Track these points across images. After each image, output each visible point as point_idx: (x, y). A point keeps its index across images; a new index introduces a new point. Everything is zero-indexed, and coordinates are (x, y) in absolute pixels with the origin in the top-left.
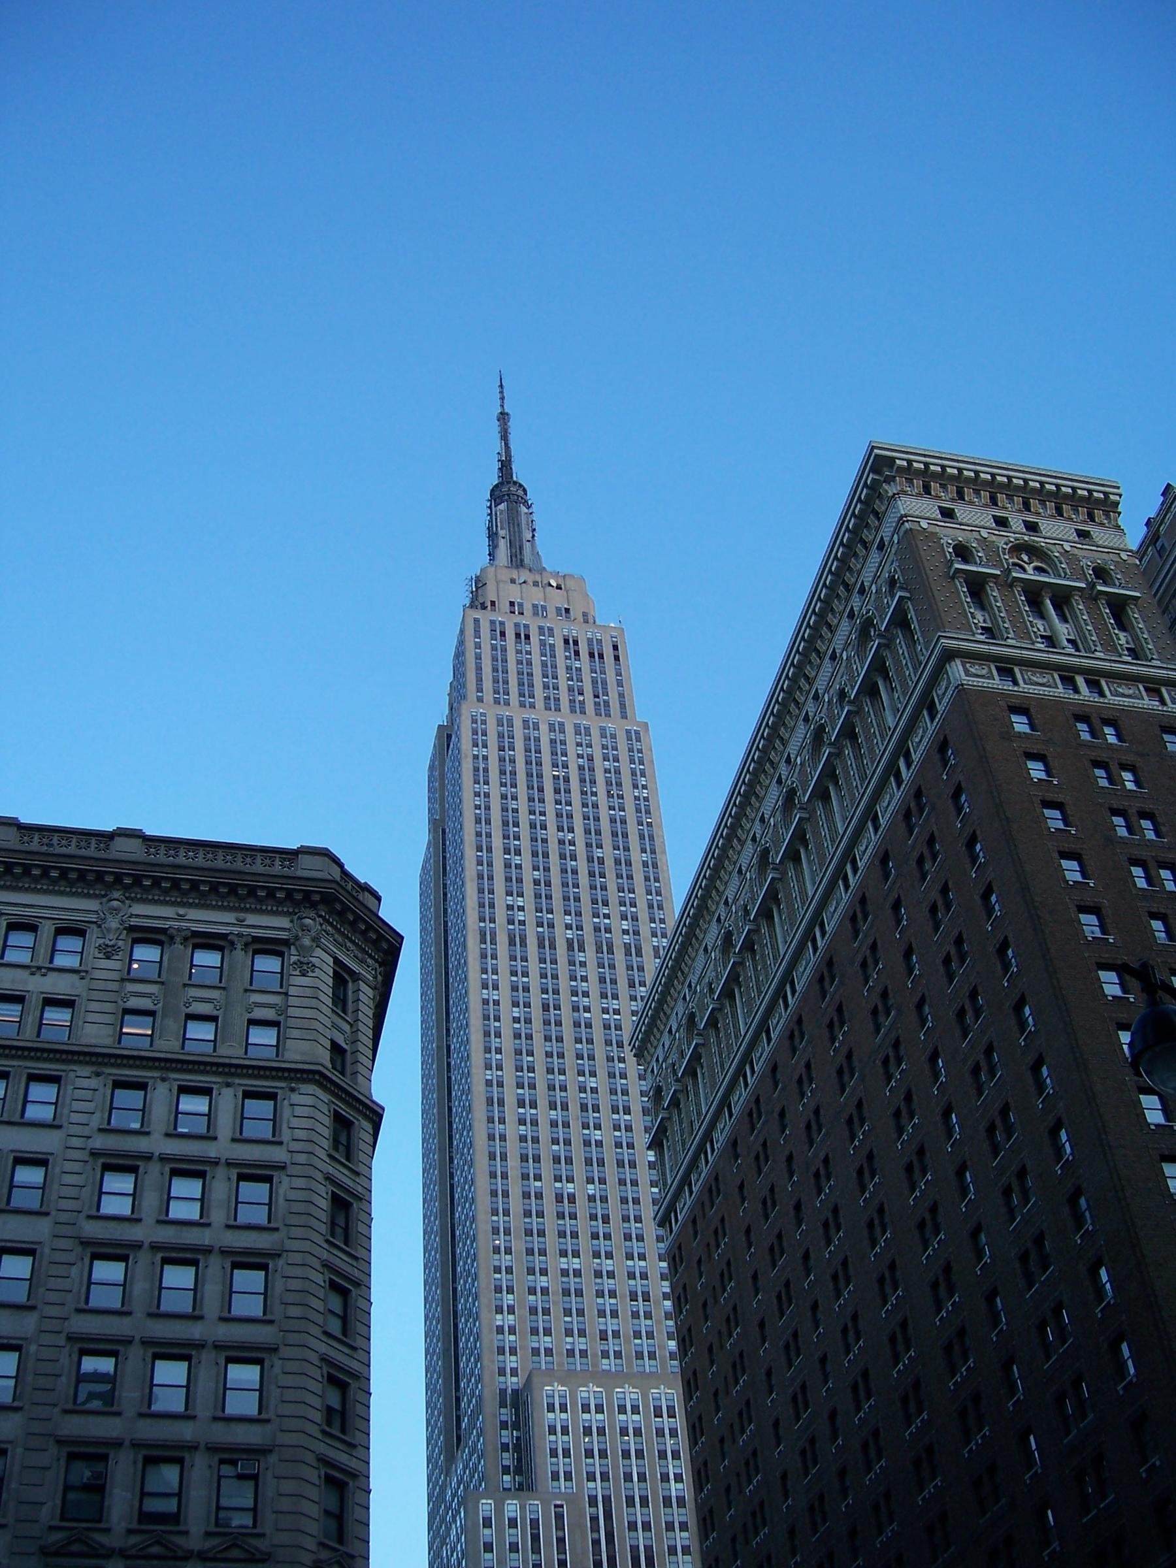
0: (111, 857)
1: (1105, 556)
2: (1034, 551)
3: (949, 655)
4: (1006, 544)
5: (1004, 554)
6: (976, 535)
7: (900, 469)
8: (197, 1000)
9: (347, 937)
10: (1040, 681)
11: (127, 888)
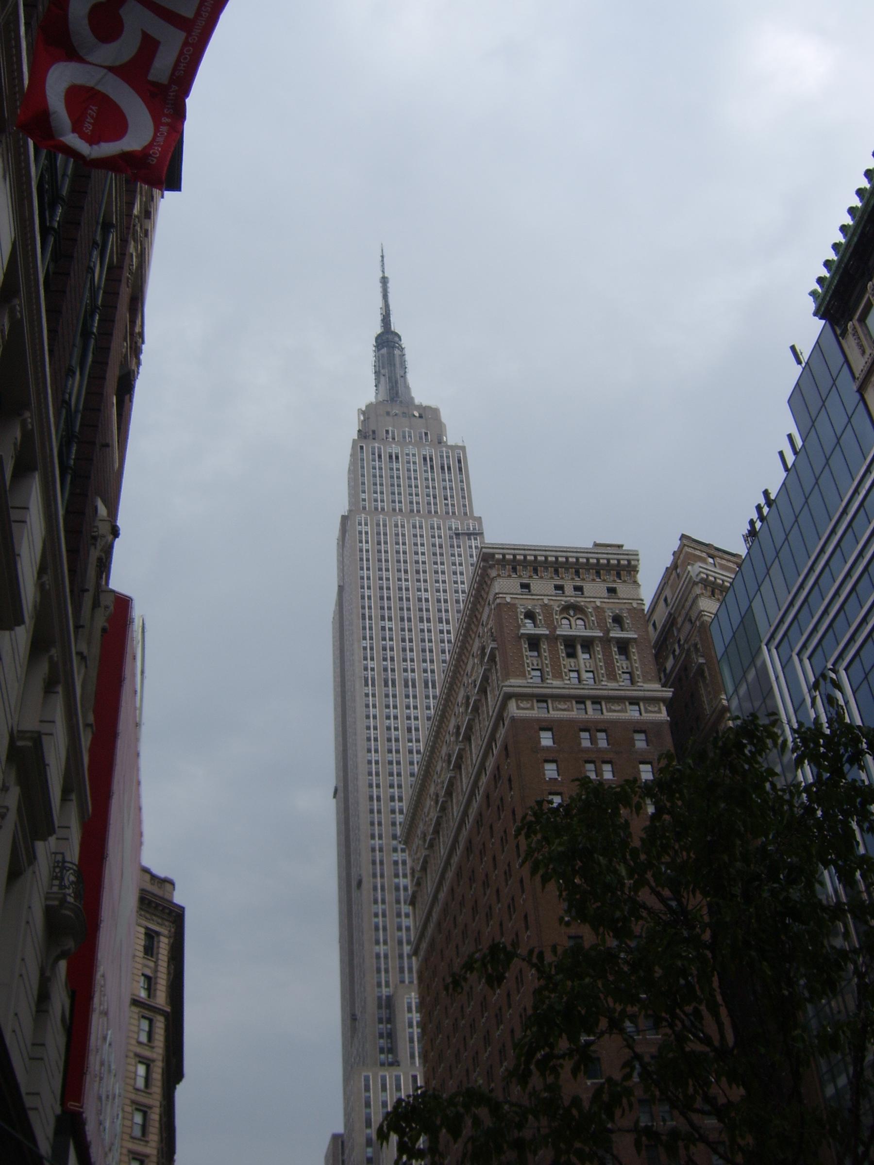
1: (623, 606)
2: (577, 609)
7: (498, 560)
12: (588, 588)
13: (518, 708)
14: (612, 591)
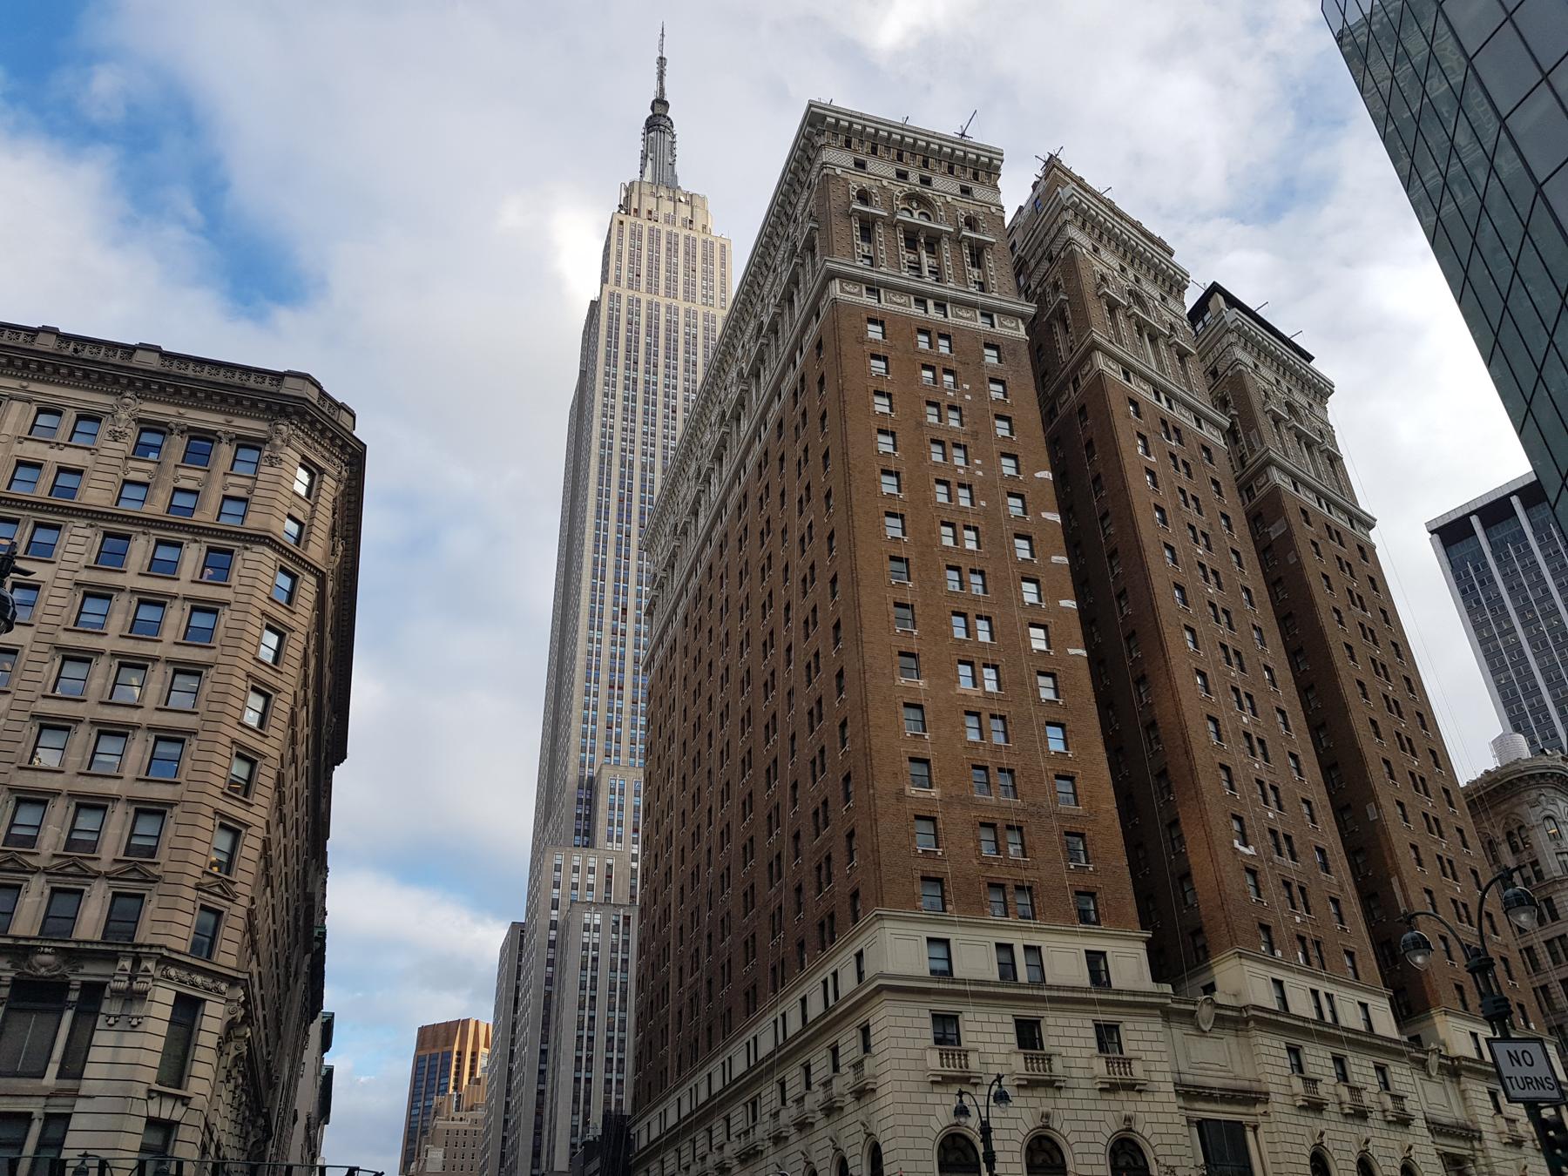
0: (131, 365)
1: (979, 209)
2: (923, 201)
3: (831, 276)
4: (901, 192)
5: (897, 200)
6: (878, 183)
8: (184, 477)
9: (317, 441)
10: (899, 301)
11: (137, 390)
12: (939, 182)
13: (842, 290)
14: (966, 191)
